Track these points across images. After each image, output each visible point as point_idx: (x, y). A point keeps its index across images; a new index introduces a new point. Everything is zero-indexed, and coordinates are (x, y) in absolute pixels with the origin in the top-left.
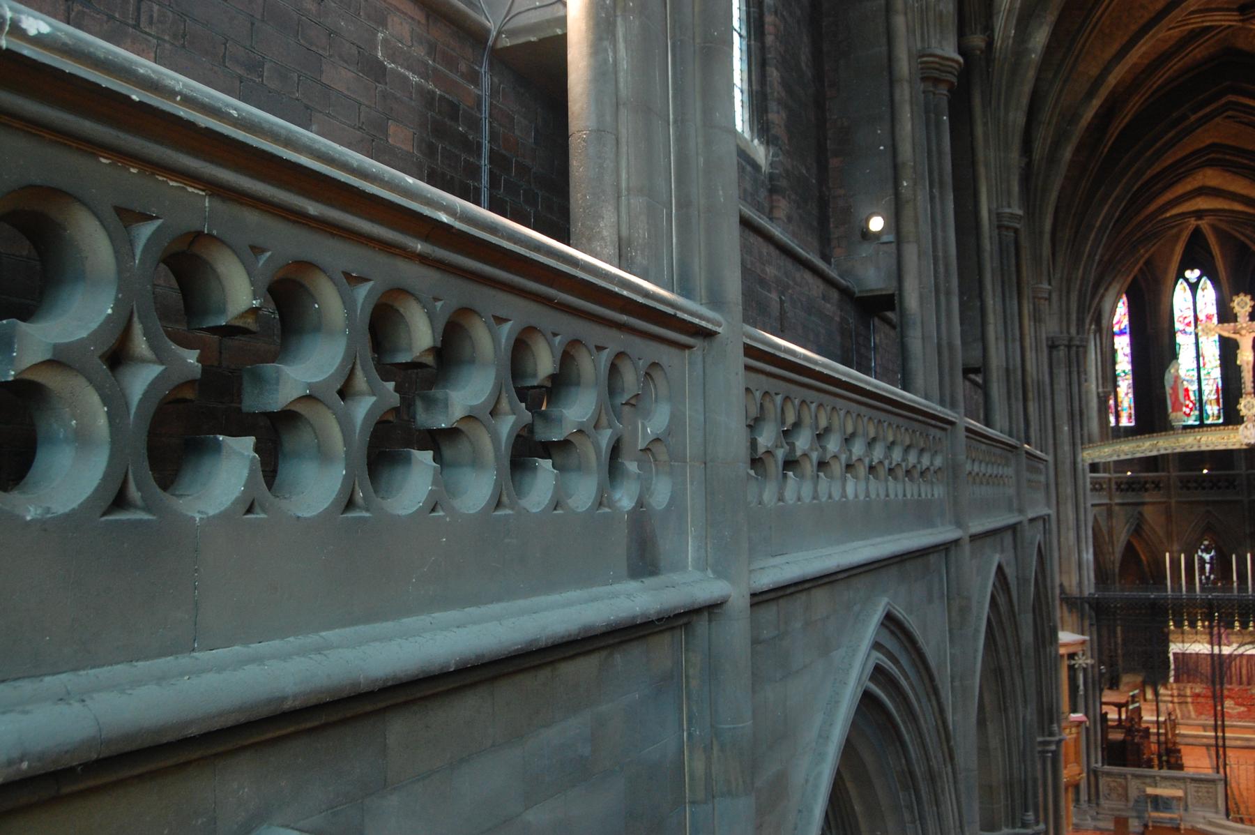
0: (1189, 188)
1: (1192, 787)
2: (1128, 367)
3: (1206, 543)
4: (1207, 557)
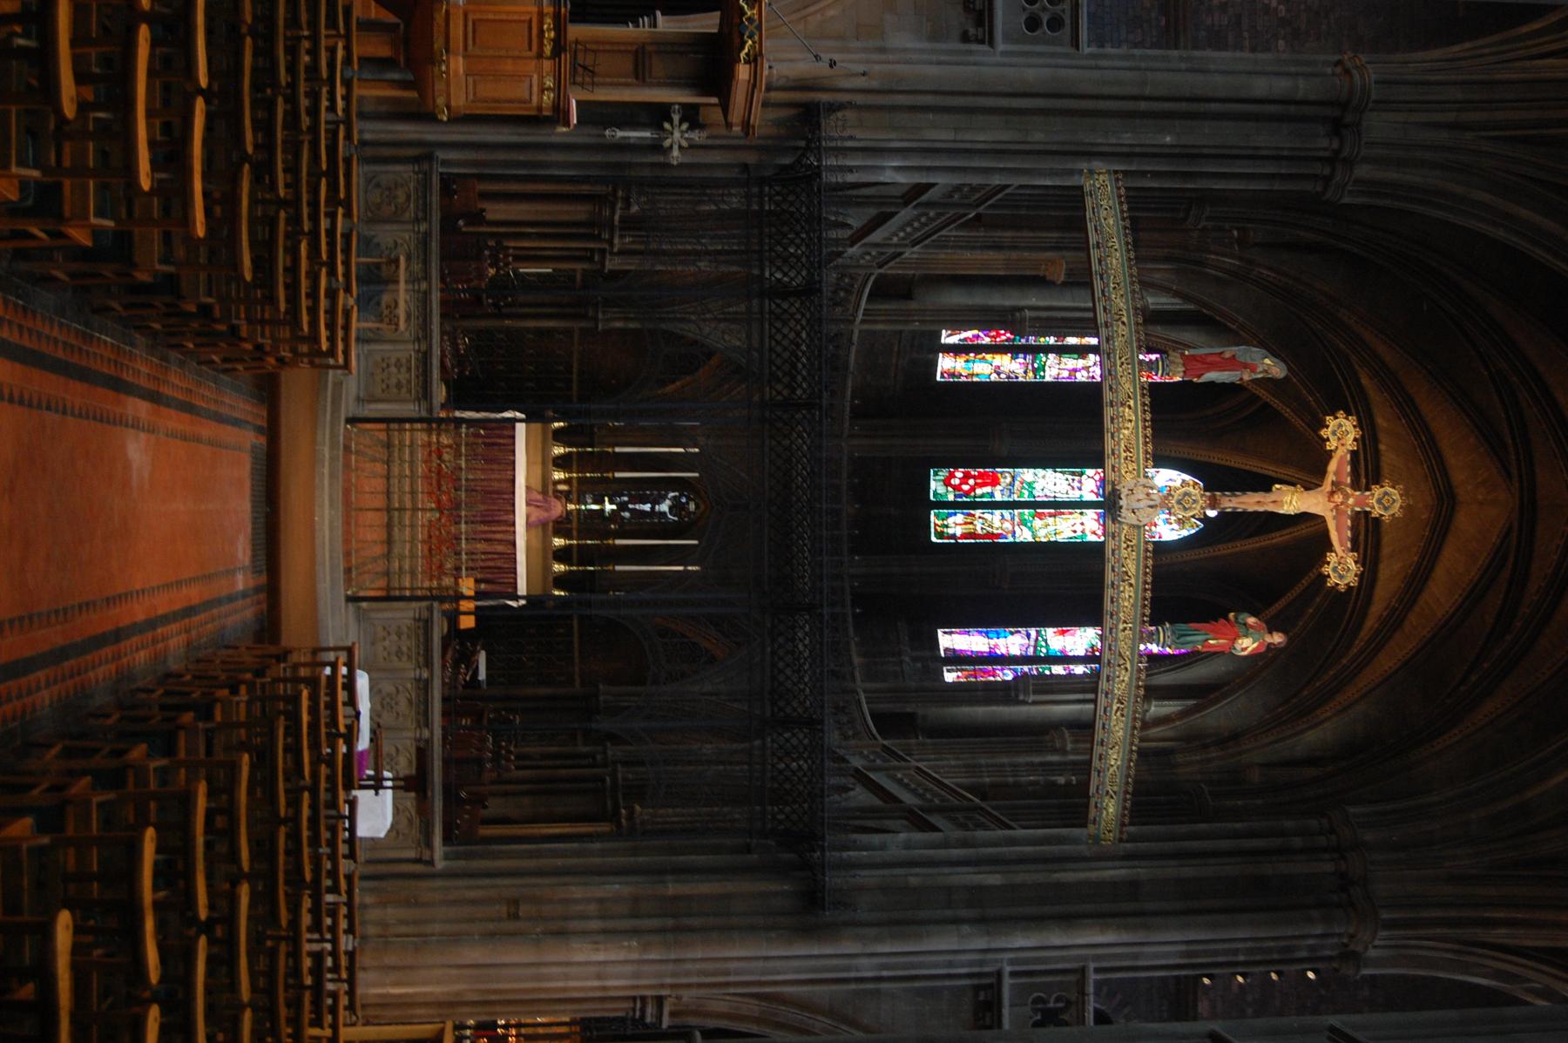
0: (1458, 477)
1: (407, 351)
2: (1050, 375)
3: (692, 507)
4: (664, 507)
